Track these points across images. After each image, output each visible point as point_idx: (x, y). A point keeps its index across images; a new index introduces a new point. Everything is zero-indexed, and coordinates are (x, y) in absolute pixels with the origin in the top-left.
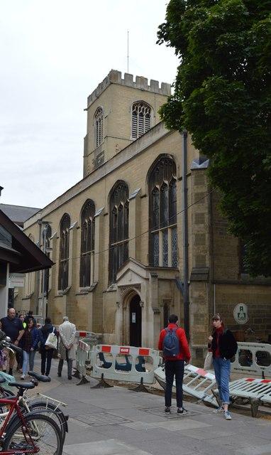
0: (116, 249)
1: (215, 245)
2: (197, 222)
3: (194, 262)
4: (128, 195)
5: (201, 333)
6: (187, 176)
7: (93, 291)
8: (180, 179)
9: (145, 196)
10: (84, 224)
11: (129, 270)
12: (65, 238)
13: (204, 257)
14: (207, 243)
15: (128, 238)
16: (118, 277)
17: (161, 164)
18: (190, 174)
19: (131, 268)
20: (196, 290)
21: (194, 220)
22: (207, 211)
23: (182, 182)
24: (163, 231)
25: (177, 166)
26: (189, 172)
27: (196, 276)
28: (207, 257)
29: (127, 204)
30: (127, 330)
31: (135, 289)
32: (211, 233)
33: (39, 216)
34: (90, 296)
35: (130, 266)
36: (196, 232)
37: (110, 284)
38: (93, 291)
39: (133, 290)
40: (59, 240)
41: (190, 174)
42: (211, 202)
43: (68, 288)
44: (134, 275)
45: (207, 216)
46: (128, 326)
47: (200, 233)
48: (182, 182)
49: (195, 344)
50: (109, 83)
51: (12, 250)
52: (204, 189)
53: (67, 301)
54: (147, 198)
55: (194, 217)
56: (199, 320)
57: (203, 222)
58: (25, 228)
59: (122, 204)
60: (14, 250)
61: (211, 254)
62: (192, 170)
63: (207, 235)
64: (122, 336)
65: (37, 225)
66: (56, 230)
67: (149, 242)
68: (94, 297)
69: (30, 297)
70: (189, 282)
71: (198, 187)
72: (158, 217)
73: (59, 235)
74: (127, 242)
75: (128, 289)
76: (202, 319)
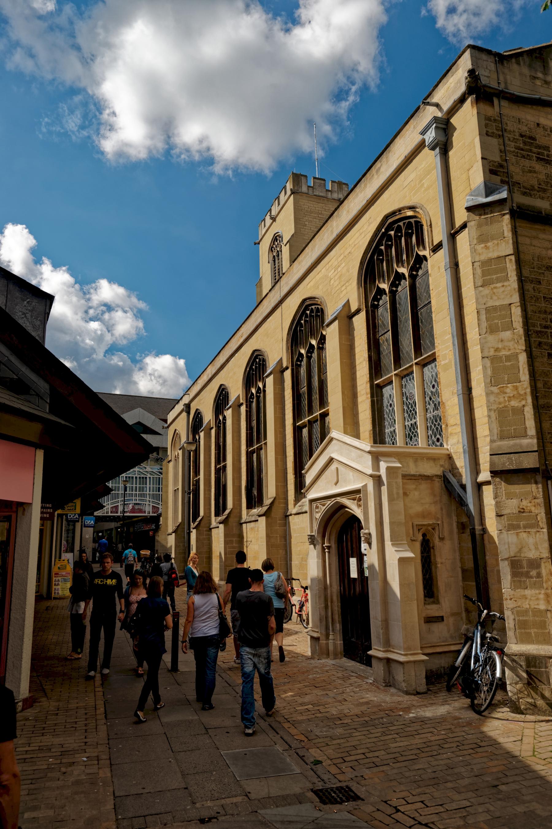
0: (305, 431)
1: (540, 385)
2: (492, 329)
3: (495, 426)
4: (323, 321)
5: (537, 612)
6: (453, 237)
7: (267, 514)
8: (436, 248)
9: (358, 311)
10: (249, 398)
11: (331, 460)
12: (221, 426)
13: (520, 411)
14: (525, 376)
15: (323, 402)
16: (308, 479)
17: (389, 238)
18: (464, 226)
19: (334, 456)
20: (510, 496)
21: (484, 324)
22: (516, 298)
23: (443, 255)
24: (401, 377)
25: (425, 228)
26: (461, 216)
27: (504, 458)
28: (529, 412)
29: (322, 341)
30: (336, 606)
31: (345, 501)
32: (531, 358)
33: (186, 400)
34: (263, 520)
35: (333, 451)
36: (492, 353)
37: (297, 499)
38: (267, 514)
39: (343, 507)
40: (213, 432)
41: (464, 226)
42: (521, 280)
43: (227, 512)
44: (342, 469)
45: (517, 312)
46: (335, 589)
47: (504, 353)
48: (443, 255)
49: (525, 639)
50: (289, 192)
51: (63, 422)
52: (507, 248)
53: (226, 536)
54: (363, 315)
55: (483, 317)
56: (527, 575)
57: (510, 326)
58: (169, 422)
59: (314, 342)
60: (63, 422)
61: (538, 408)
62: (469, 209)
63: (523, 358)
64: (323, 613)
65: (184, 414)
66: (208, 416)
67: (373, 402)
68: (269, 526)
69: (175, 532)
70: (484, 475)
71: (487, 248)
72: (387, 347)
73: (213, 424)
74: (325, 415)
75: (329, 503)
76: (534, 573)
